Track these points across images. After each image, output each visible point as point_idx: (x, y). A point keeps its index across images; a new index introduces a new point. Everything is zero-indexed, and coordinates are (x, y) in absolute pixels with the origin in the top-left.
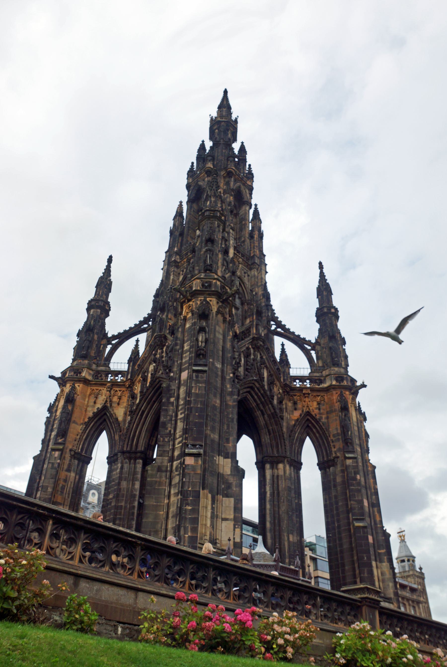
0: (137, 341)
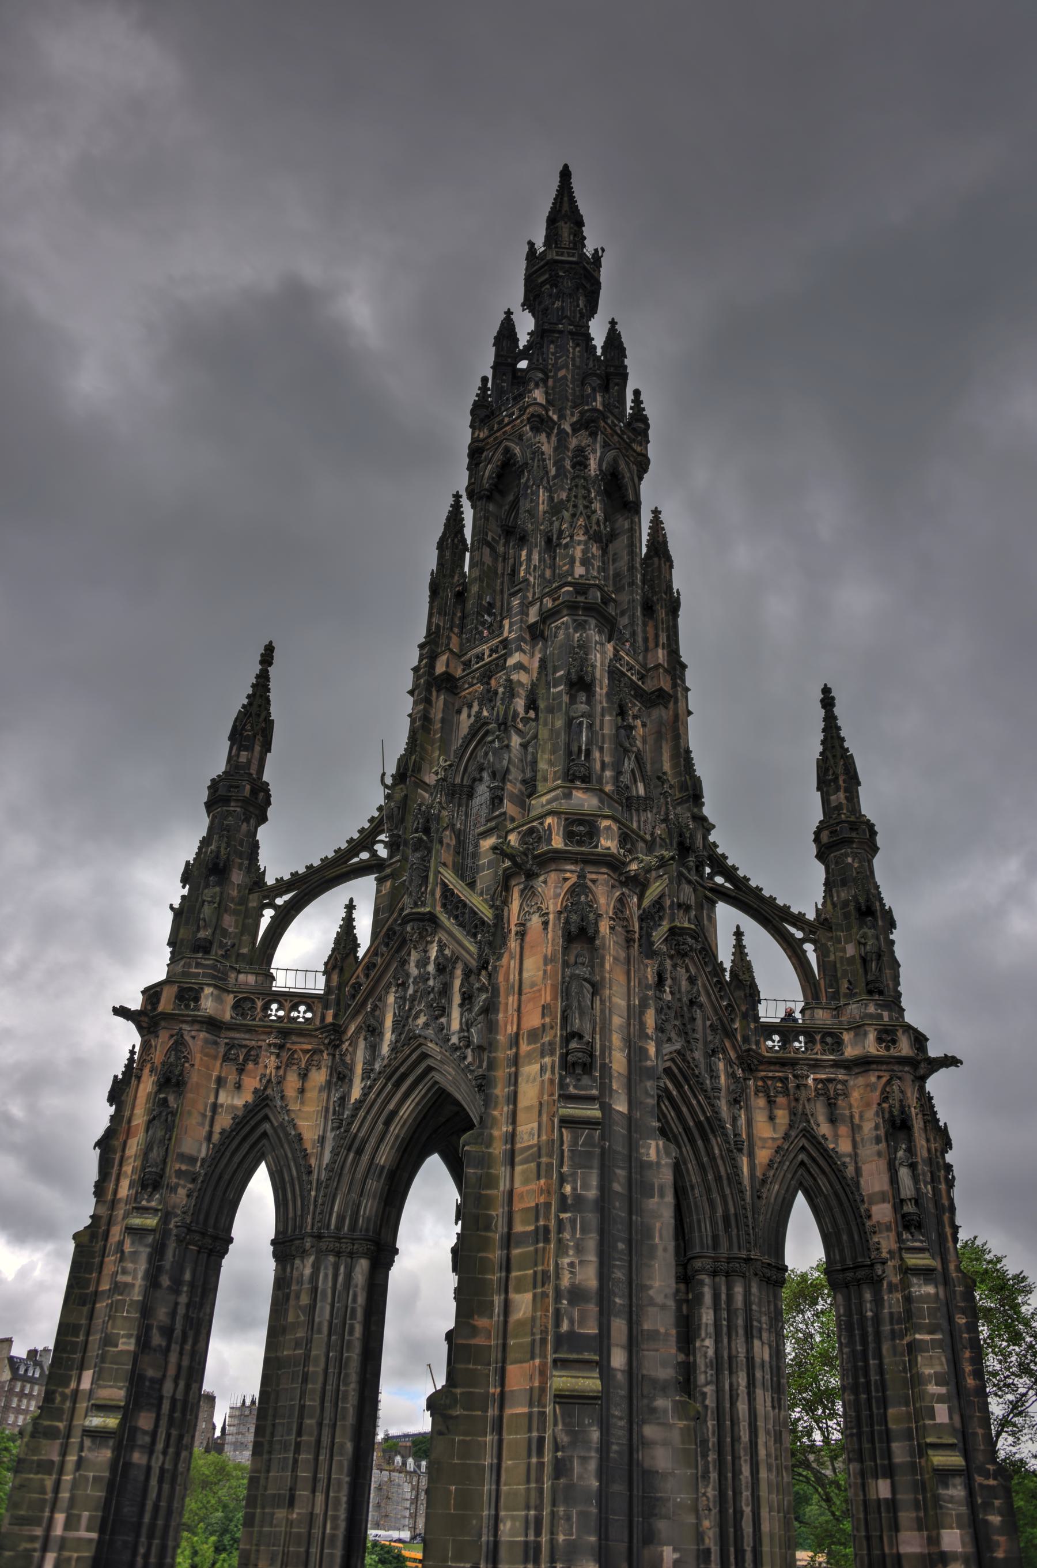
0: (350, 907)
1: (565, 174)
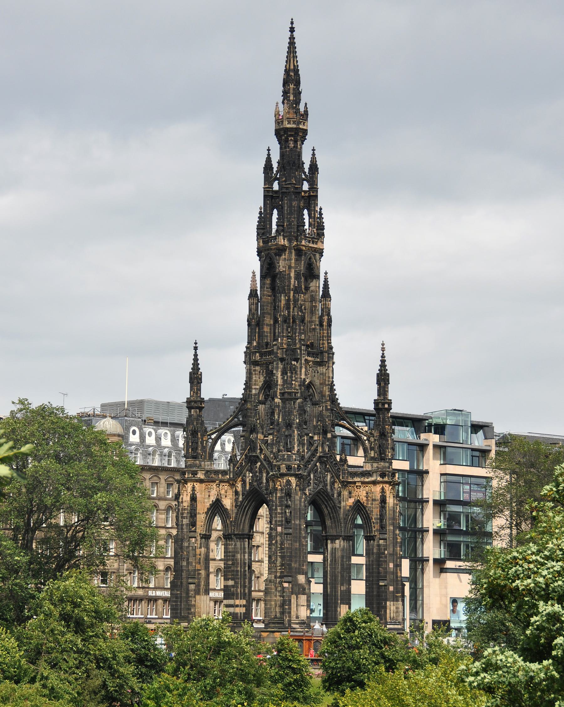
1: (292, 30)
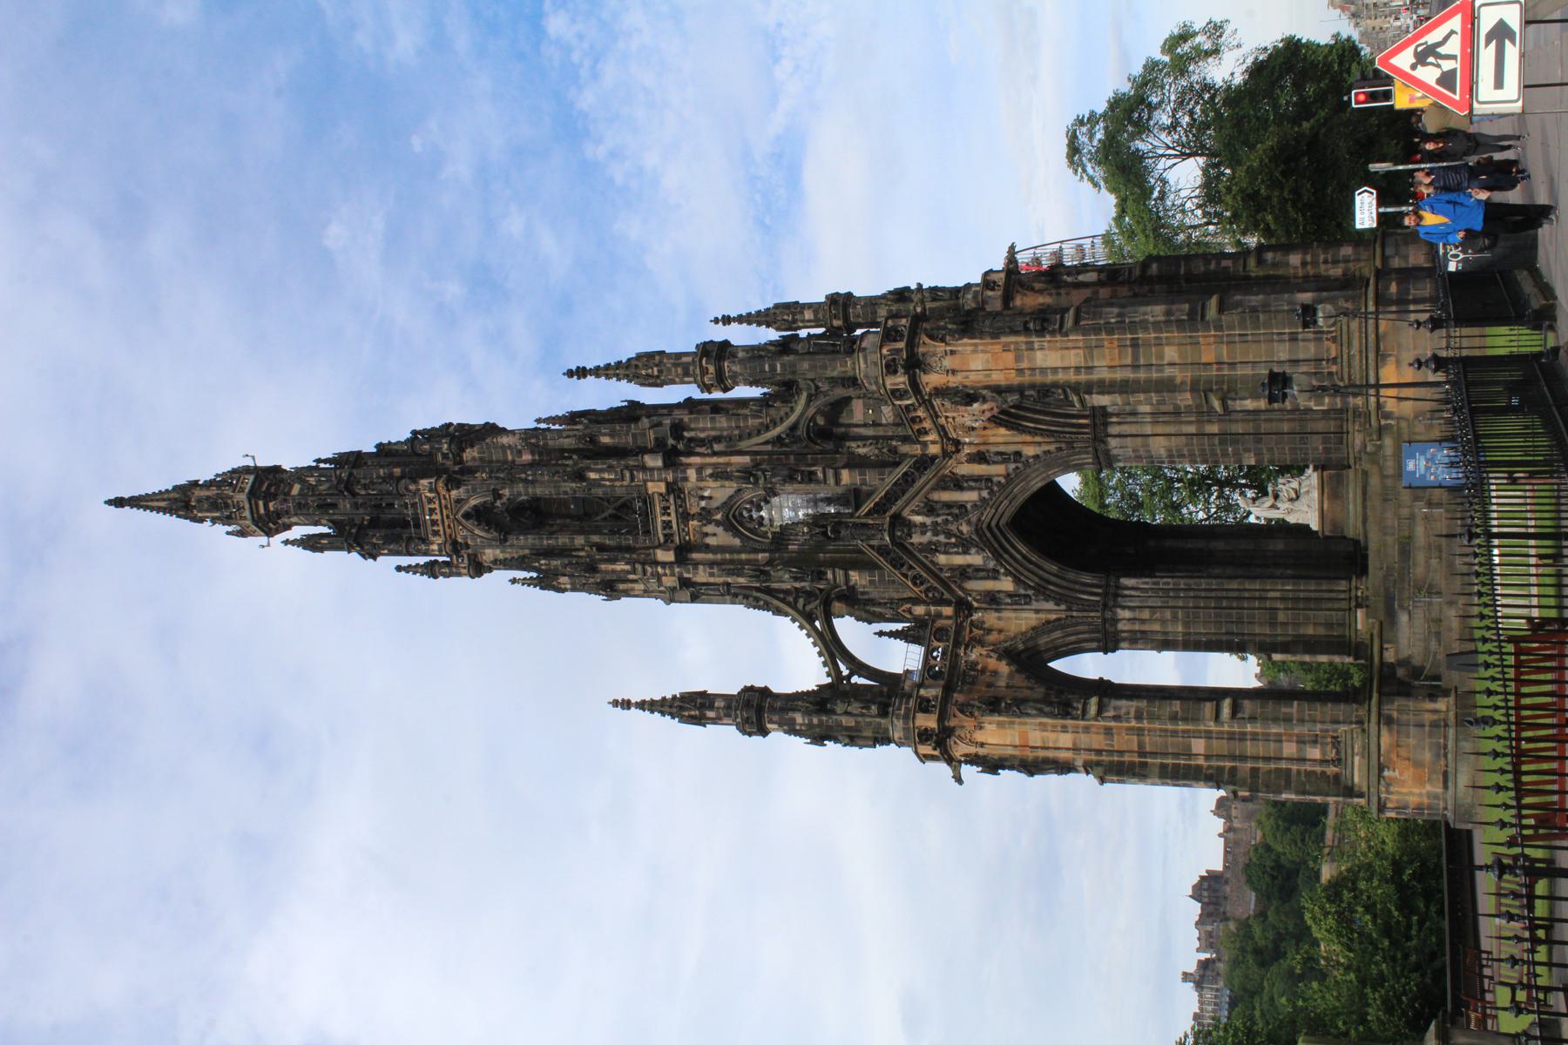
1: (119, 502)
